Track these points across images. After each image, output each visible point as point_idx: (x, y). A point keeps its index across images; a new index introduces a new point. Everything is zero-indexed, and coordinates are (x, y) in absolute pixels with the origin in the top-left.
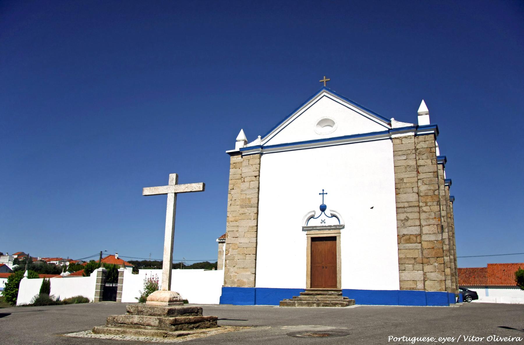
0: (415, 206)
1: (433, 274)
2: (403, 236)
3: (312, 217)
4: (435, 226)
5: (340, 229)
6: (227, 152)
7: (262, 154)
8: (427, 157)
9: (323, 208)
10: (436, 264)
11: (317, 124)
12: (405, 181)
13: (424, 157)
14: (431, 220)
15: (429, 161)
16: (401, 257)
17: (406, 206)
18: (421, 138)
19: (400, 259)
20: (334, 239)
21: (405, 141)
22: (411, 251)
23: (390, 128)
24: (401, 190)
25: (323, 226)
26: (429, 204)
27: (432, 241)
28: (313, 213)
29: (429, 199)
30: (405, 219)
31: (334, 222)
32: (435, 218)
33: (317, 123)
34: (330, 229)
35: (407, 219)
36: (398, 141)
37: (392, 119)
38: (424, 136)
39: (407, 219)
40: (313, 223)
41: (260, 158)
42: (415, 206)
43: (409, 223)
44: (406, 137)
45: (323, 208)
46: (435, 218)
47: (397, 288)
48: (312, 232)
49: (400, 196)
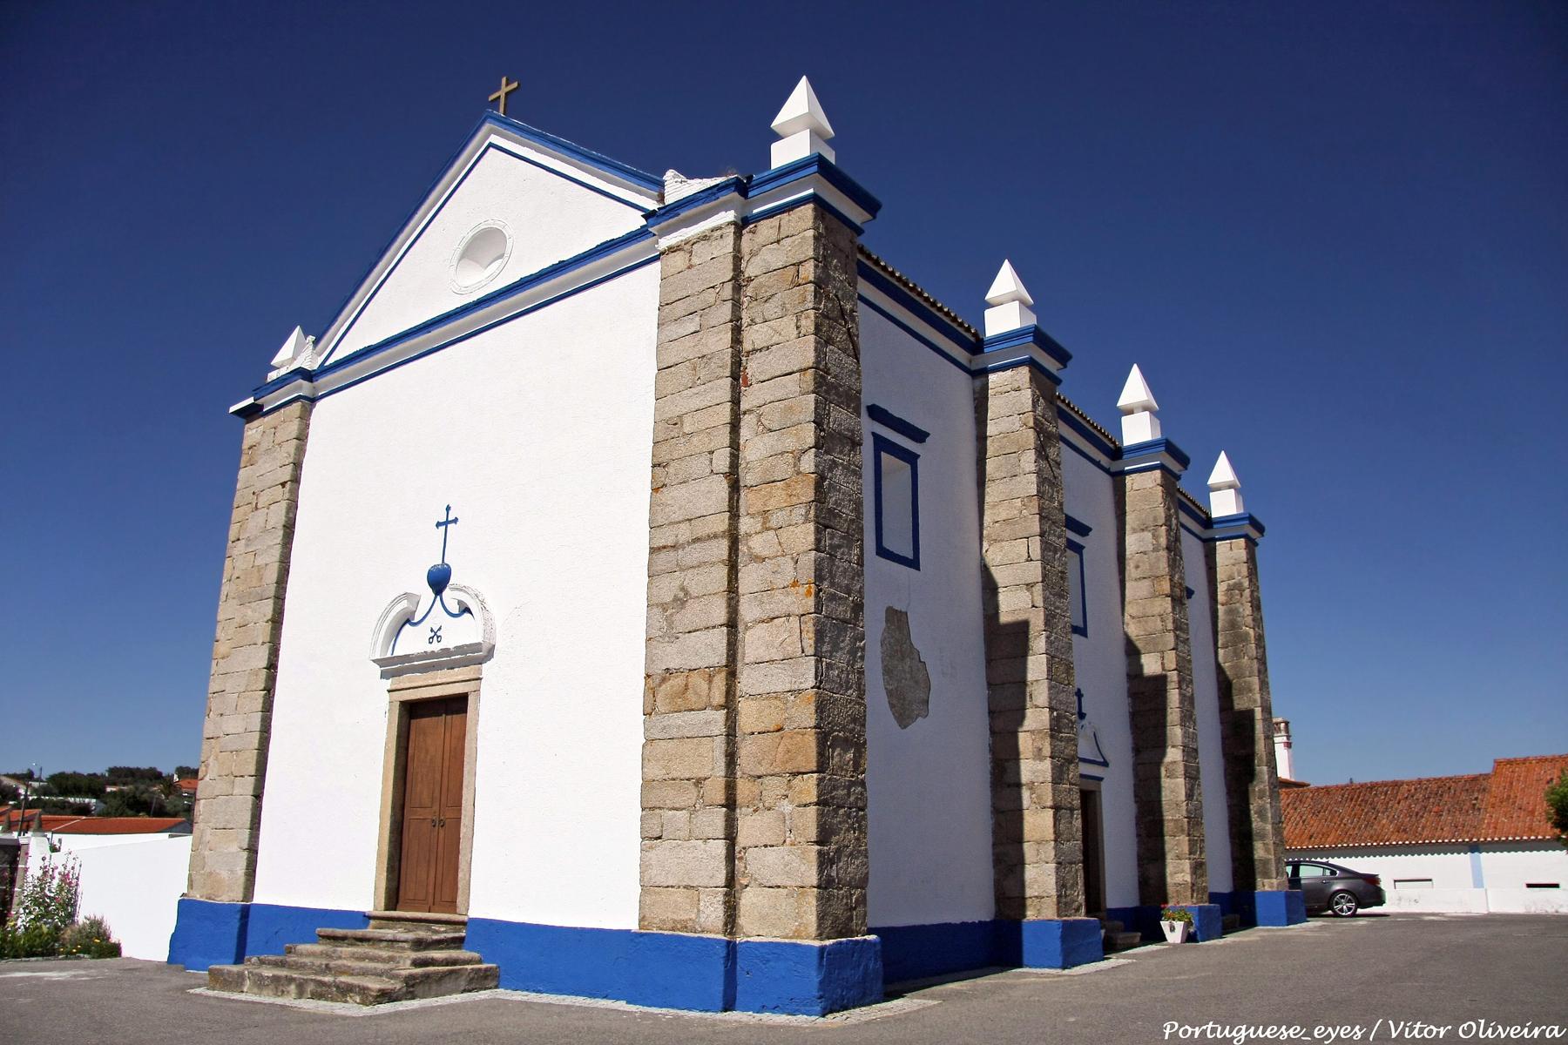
0: (715, 536)
1: (771, 856)
2: (664, 680)
3: (408, 621)
4: (794, 621)
5: (481, 661)
6: (233, 409)
7: (313, 401)
8: (783, 306)
9: (439, 580)
10: (787, 807)
11: (463, 256)
12: (687, 430)
13: (771, 309)
14: (778, 595)
15: (788, 325)
16: (650, 776)
17: (682, 540)
18: (766, 229)
19: (647, 785)
20: (457, 705)
21: (702, 253)
22: (690, 744)
23: (652, 205)
24: (671, 470)
25: (433, 655)
26: (773, 523)
27: (776, 696)
28: (404, 604)
29: (778, 495)
30: (676, 599)
31: (459, 633)
32: (795, 584)
33: (459, 252)
34: (451, 666)
35: (681, 601)
36: (678, 260)
37: (670, 175)
38: (774, 221)
39: (681, 601)
40: (413, 642)
41: (305, 417)
42: (715, 536)
43: (687, 618)
44: (704, 238)
45: (439, 580)
46: (795, 584)
47: (626, 919)
48: (406, 680)
49: (666, 495)
